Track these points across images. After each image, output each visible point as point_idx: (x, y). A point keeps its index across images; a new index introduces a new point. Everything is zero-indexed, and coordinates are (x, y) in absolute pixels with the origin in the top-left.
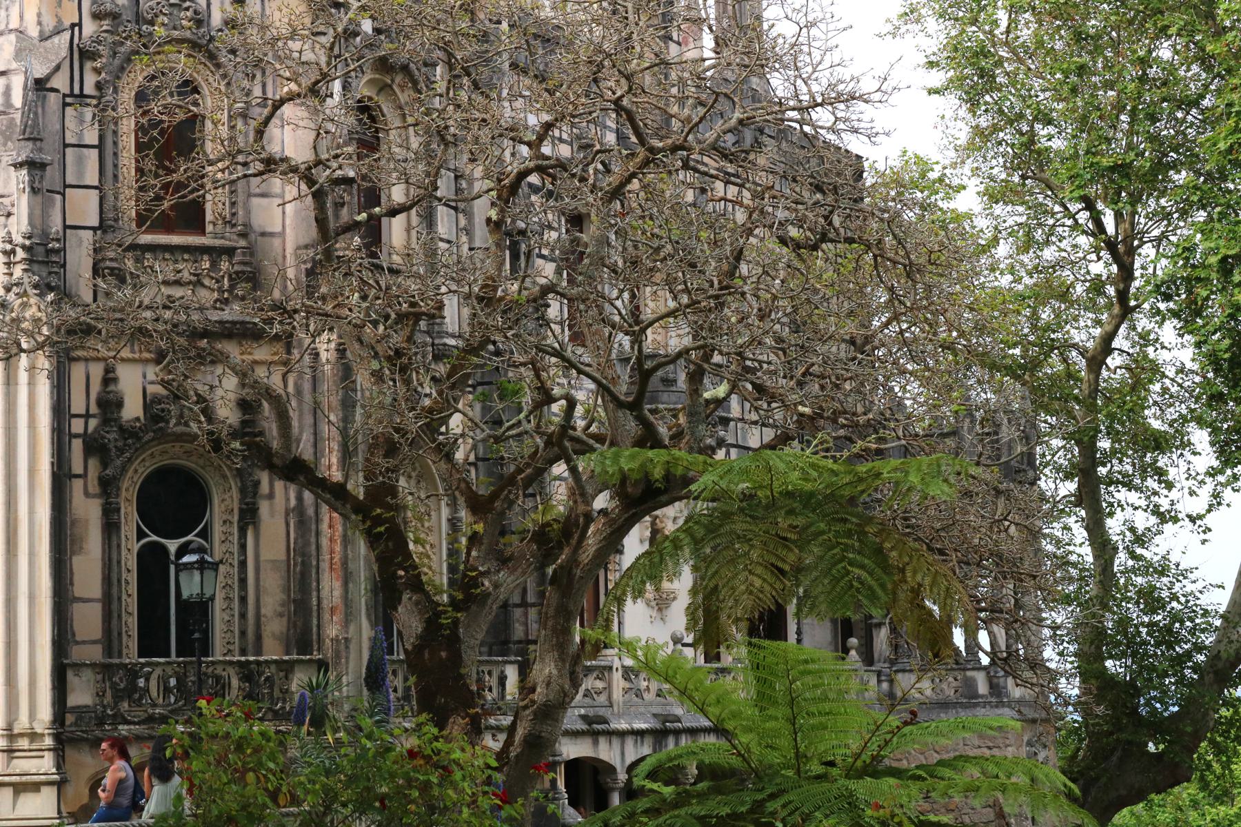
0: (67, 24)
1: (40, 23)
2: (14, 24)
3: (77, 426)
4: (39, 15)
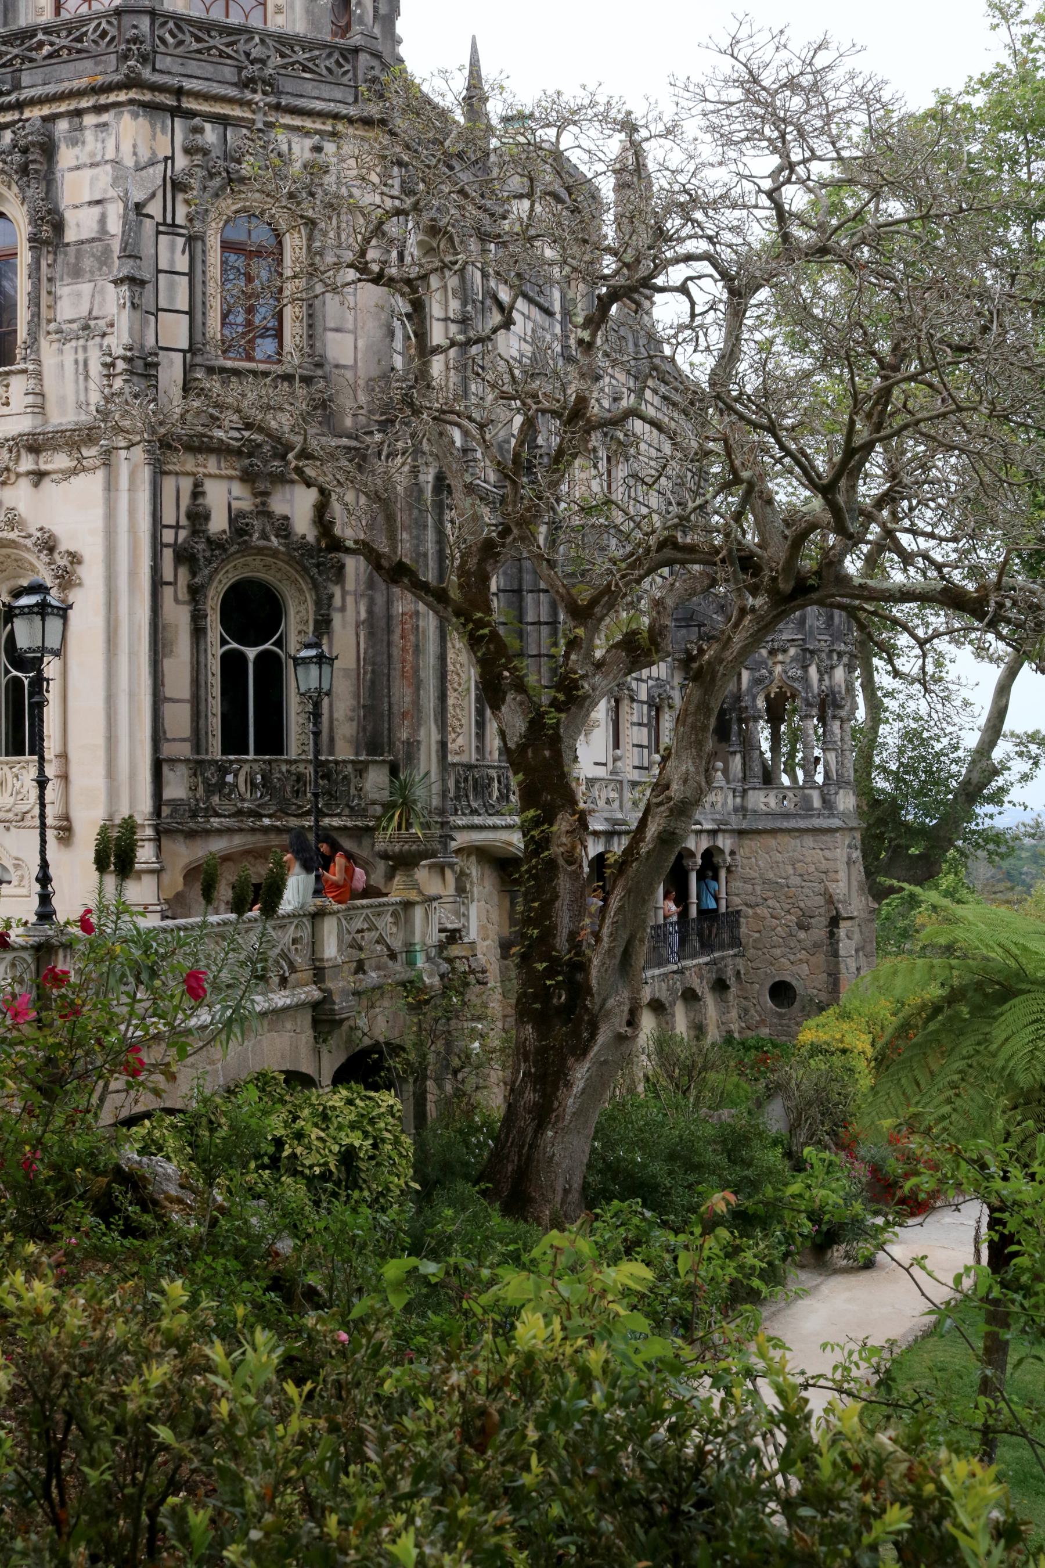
0: (161, 156)
1: (135, 154)
2: (110, 155)
3: (168, 536)
4: (135, 146)
